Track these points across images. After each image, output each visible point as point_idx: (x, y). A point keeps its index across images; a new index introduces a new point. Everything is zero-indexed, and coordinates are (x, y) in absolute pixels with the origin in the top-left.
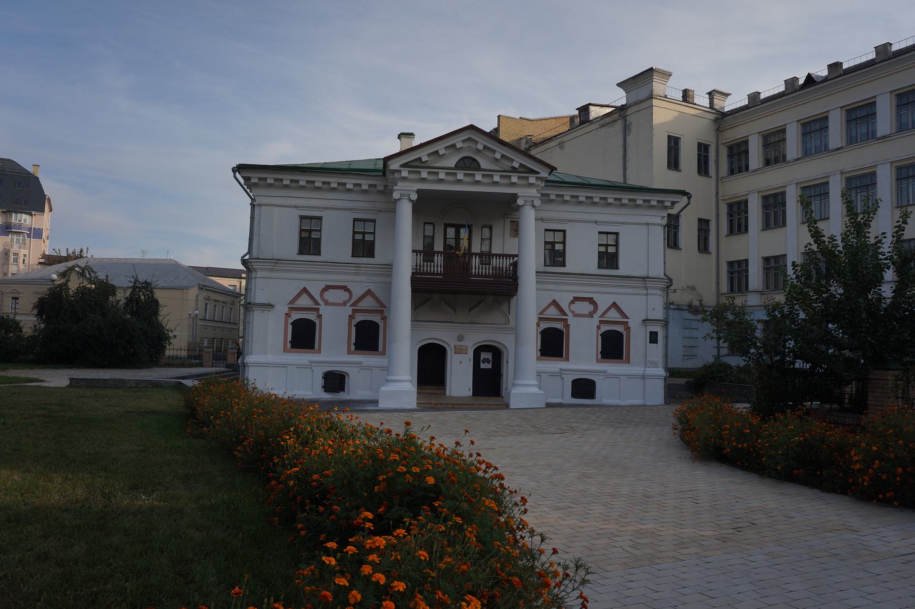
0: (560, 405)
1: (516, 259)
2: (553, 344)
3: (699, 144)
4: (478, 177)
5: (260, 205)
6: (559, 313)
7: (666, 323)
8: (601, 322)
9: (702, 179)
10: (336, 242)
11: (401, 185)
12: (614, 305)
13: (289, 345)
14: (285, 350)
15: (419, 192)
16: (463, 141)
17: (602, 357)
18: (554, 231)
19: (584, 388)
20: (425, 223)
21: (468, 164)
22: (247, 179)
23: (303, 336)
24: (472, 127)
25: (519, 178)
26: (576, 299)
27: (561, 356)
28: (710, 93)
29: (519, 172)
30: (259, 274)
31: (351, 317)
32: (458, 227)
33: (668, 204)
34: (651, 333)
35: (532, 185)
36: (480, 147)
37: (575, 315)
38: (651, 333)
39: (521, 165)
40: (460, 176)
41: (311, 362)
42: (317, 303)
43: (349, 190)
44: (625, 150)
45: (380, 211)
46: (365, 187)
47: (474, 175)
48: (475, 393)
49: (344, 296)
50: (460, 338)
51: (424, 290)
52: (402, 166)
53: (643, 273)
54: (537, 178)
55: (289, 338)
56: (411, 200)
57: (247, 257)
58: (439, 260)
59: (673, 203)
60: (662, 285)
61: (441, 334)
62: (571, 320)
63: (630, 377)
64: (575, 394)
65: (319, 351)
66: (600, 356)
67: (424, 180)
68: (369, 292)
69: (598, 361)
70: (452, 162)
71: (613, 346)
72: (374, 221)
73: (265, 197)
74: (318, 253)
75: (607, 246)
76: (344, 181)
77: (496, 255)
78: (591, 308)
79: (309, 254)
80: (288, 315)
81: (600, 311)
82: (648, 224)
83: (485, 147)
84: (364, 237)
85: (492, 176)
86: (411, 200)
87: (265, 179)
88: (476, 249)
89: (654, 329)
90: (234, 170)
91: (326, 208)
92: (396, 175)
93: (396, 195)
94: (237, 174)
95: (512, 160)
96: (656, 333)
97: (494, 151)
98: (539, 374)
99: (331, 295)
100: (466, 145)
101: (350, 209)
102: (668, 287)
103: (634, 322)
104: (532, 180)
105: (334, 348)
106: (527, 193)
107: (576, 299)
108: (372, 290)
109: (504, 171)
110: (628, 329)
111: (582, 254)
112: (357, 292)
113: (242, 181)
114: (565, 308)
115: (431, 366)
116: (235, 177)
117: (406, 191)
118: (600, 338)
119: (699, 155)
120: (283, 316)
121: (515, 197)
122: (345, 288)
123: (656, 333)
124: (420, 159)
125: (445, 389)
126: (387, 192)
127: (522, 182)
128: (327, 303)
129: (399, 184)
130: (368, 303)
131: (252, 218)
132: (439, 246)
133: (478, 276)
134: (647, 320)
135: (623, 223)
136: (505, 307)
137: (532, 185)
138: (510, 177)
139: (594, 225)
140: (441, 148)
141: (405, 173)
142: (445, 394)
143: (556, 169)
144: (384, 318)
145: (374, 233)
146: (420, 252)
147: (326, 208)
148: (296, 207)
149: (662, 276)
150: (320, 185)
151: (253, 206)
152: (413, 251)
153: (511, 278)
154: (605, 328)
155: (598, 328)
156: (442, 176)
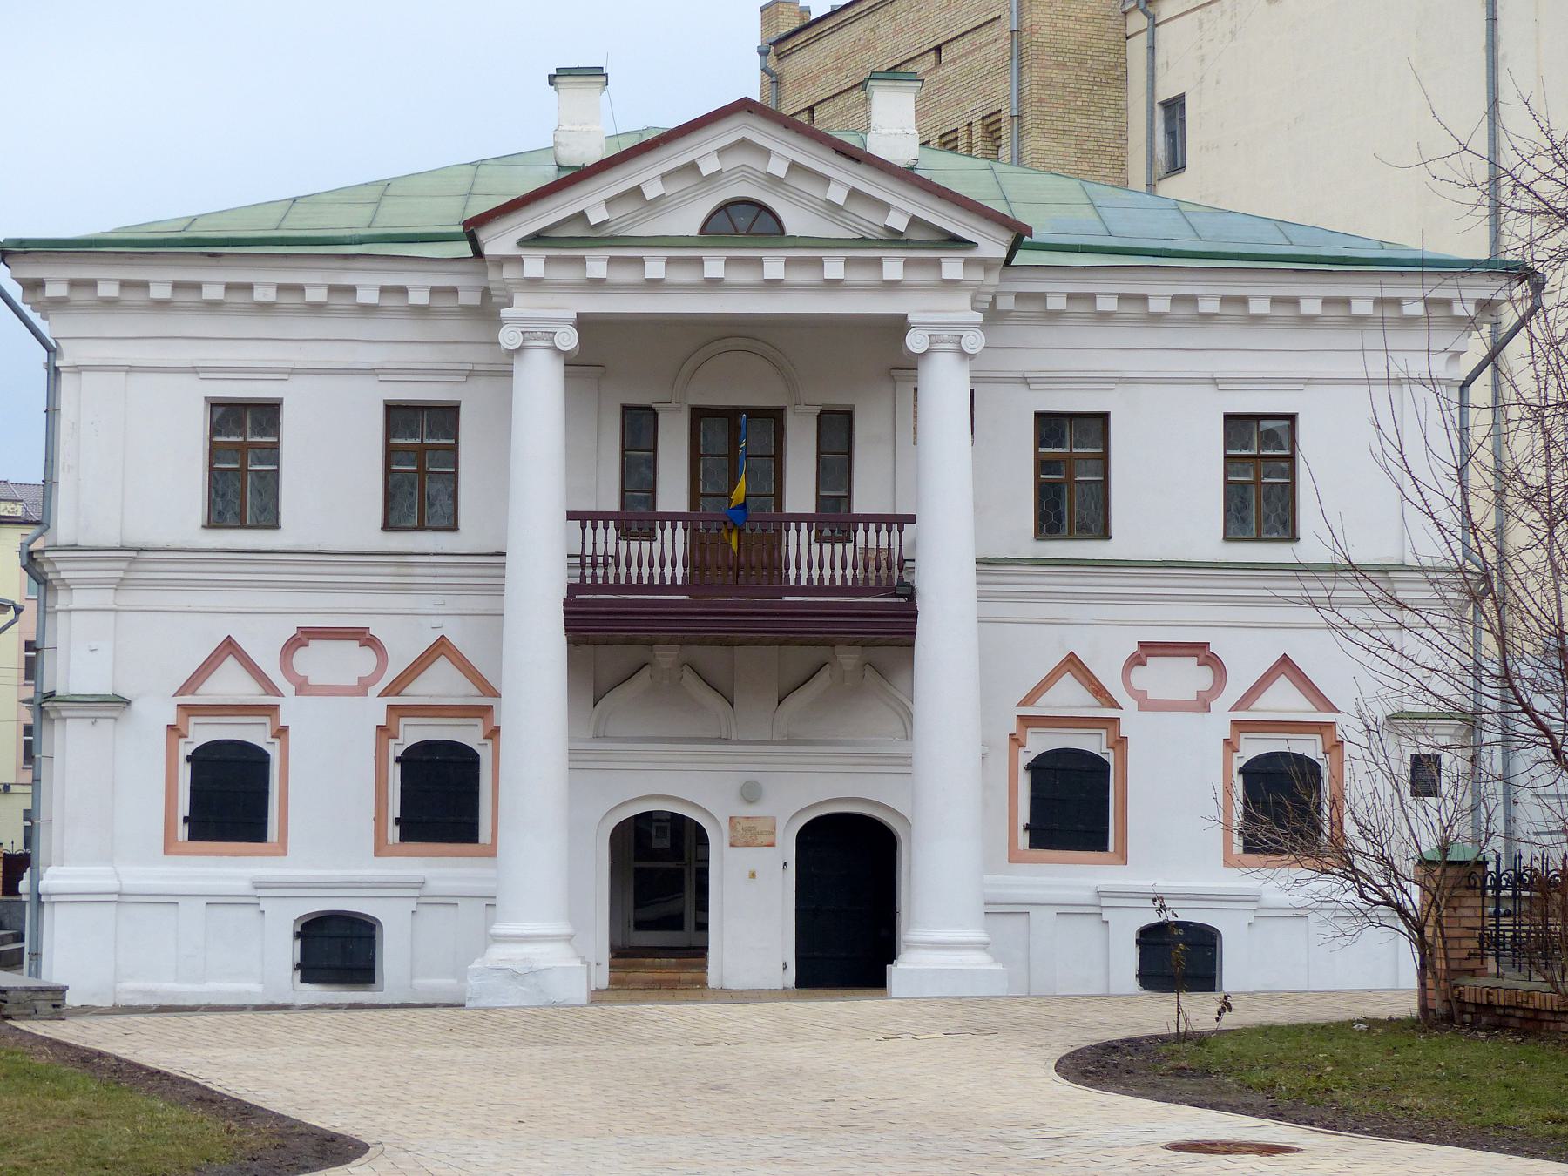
2: (1070, 804)
4: (774, 268)
5: (78, 369)
6: (1089, 699)
7: (1471, 721)
11: (523, 306)
14: (169, 847)
15: (584, 323)
21: (744, 223)
22: (33, 287)
23: (229, 796)
26: (1149, 649)
27: (1103, 846)
30: (80, 598)
35: (952, 284)
36: (778, 168)
37: (1146, 704)
39: (914, 221)
40: (714, 267)
41: (259, 884)
42: (270, 687)
44: (1492, 20)
45: (471, 374)
46: (419, 298)
47: (759, 262)
49: (359, 661)
50: (751, 794)
52: (526, 242)
54: (968, 262)
55: (184, 808)
56: (557, 351)
62: (1132, 722)
68: (441, 648)
70: (688, 219)
74: (274, 524)
76: (347, 279)
78: (1203, 677)
79: (243, 525)
86: (557, 351)
87: (92, 284)
91: (293, 371)
92: (509, 273)
93: (509, 337)
95: (886, 207)
98: (998, 910)
99: (317, 661)
100: (733, 161)
101: (372, 372)
104: (952, 268)
106: (939, 313)
107: (1149, 649)
109: (863, 242)
112: (403, 647)
114: (1112, 682)
115: (657, 885)
117: (546, 312)
121: (899, 325)
122: (361, 636)
124: (582, 215)
126: (487, 312)
127: (920, 276)
128: (303, 687)
129: (519, 299)
130: (441, 684)
131: (52, 412)
135: (1309, 381)
139: (1208, 391)
140: (648, 175)
141: (534, 265)
142: (704, 983)
143: (1028, 231)
144: (494, 733)
148: (193, 370)
150: (270, 295)
151: (54, 373)
152: (571, 516)
154: (1254, 747)
156: (655, 268)
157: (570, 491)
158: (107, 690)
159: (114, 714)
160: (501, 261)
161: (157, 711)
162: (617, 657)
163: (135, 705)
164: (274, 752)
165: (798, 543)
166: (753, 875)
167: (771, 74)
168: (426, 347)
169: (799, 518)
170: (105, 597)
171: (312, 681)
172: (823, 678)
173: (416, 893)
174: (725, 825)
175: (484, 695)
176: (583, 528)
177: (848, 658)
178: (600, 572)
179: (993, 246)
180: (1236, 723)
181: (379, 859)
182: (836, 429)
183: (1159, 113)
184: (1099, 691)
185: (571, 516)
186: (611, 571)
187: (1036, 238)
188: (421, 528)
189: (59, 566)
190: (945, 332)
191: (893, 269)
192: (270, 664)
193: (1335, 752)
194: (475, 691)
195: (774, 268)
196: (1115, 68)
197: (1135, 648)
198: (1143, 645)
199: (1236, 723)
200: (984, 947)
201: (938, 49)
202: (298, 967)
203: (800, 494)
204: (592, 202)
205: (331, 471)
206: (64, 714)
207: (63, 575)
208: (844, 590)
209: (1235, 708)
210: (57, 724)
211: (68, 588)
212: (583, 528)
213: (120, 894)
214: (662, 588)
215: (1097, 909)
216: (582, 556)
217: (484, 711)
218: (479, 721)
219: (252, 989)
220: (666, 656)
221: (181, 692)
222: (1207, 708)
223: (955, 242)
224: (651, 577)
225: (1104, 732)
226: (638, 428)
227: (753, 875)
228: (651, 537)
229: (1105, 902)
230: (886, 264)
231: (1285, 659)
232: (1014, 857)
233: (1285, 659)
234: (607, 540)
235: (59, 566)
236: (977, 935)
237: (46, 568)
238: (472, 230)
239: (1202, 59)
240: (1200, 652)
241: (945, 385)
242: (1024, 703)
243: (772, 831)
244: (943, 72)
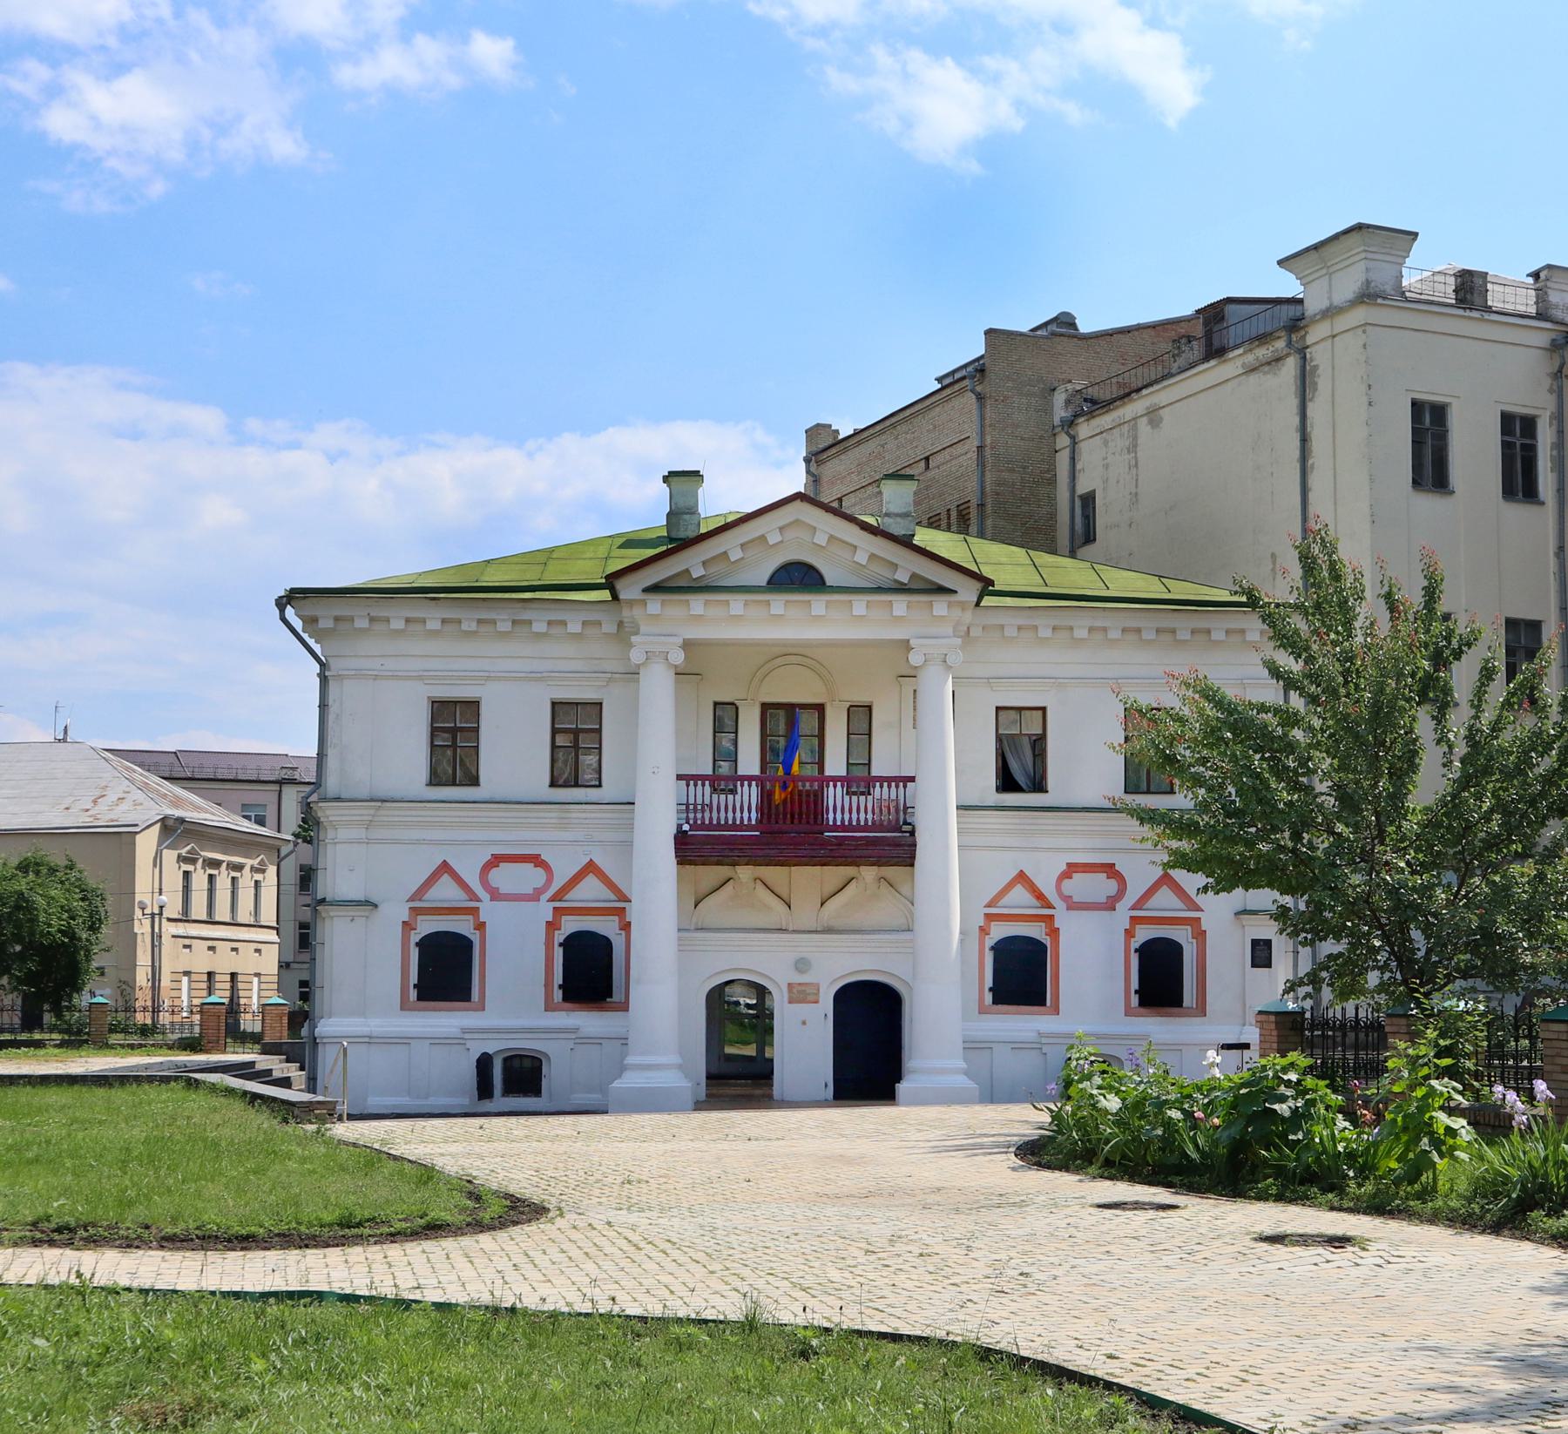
3: (1507, 419)
6: (1035, 902)
8: (1135, 920)
9: (1518, 513)
13: (413, 994)
14: (405, 1006)
17: (1142, 1004)
18: (1020, 709)
21: (798, 578)
22: (310, 622)
23: (445, 970)
27: (1042, 1003)
28: (1536, 275)
30: (343, 834)
31: (552, 926)
34: (1255, 943)
36: (821, 539)
38: (1255, 943)
39: (914, 576)
41: (464, 1031)
43: (539, 636)
44: (1304, 439)
49: (536, 877)
54: (950, 605)
55: (414, 978)
61: (766, 960)
65: (482, 1007)
66: (1135, 1000)
68: (590, 868)
74: (474, 781)
78: (1111, 887)
80: (407, 926)
93: (636, 656)
94: (290, 612)
96: (1268, 943)
99: (504, 877)
104: (940, 605)
105: (514, 998)
108: (598, 861)
113: (298, 624)
114: (1049, 890)
116: (284, 620)
119: (1506, 446)
120: (398, 930)
122: (536, 860)
123: (1268, 943)
128: (495, 895)
130: (590, 891)
131: (323, 706)
134: (1245, 912)
142: (770, 1097)
143: (991, 583)
144: (626, 927)
148: (420, 678)
154: (1144, 934)
155: (1129, 934)
157: (678, 760)
160: (631, 603)
162: (710, 874)
164: (475, 937)
165: (834, 796)
166: (804, 1023)
167: (813, 475)
169: (835, 779)
170: (361, 833)
174: (785, 989)
177: (869, 873)
178: (699, 815)
182: (861, 717)
183: (1078, 503)
184: (1040, 896)
185: (679, 777)
186: (707, 815)
187: (997, 588)
196: (1048, 471)
197: (1064, 867)
198: (1069, 865)
201: (927, 459)
203: (835, 764)
205: (514, 750)
208: (866, 828)
209: (1133, 908)
210: (327, 922)
214: (741, 827)
216: (687, 805)
217: (620, 912)
220: (745, 873)
221: (411, 899)
223: (942, 590)
226: (725, 717)
228: (733, 792)
230: (895, 605)
234: (704, 793)
238: (611, 582)
239: (1106, 467)
243: (817, 994)
244: (930, 474)
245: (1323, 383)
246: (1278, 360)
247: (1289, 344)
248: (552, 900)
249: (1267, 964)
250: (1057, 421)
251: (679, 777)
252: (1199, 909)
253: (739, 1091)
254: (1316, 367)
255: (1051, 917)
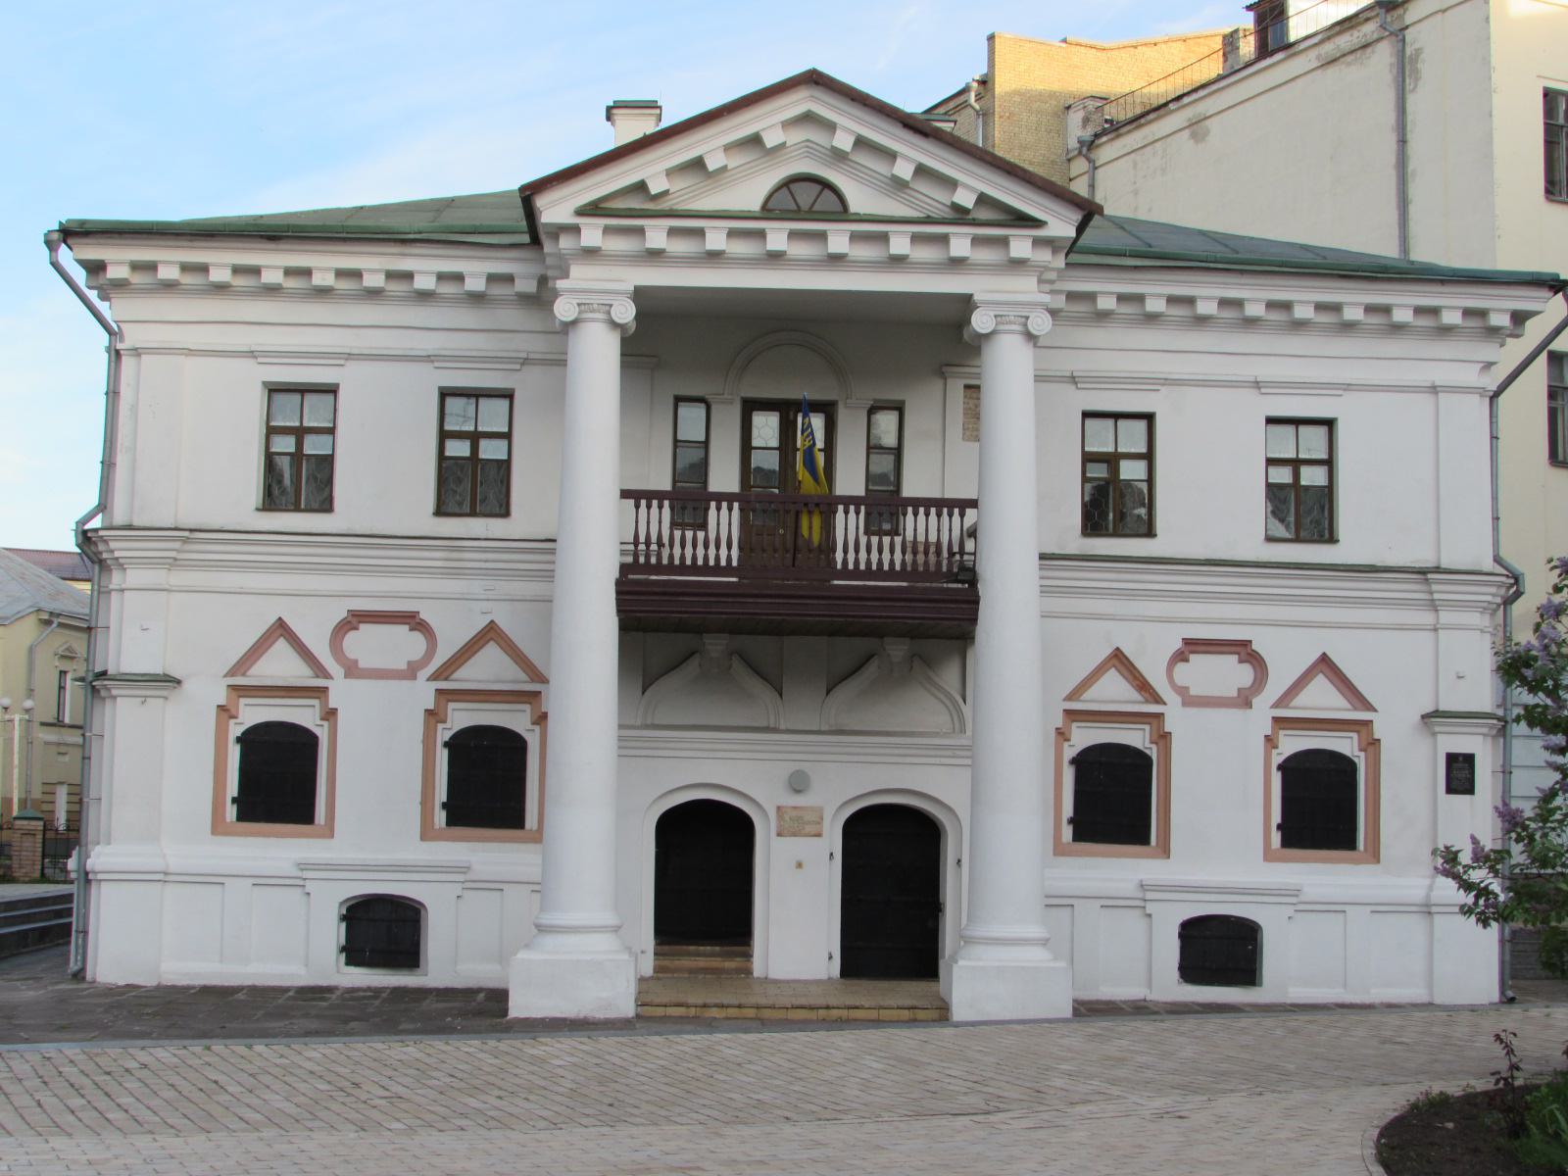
0: (1140, 1009)
1: (971, 515)
2: (1114, 798)
5: (137, 352)
6: (1135, 695)
10: (385, 468)
11: (581, 275)
12: (1325, 664)
13: (231, 812)
14: (218, 827)
16: (787, 124)
18: (1117, 416)
19: (1220, 949)
20: (679, 400)
22: (95, 268)
23: (277, 778)
24: (814, 79)
25: (977, 241)
26: (1194, 646)
29: (975, 223)
30: (134, 577)
31: (433, 716)
32: (788, 411)
33: (1501, 320)
34: (1452, 759)
35: (1018, 264)
36: (844, 141)
37: (1189, 700)
38: (1452, 759)
39: (983, 200)
41: (303, 866)
42: (320, 670)
43: (425, 296)
44: (1402, 142)
45: (526, 362)
47: (822, 236)
48: (846, 972)
50: (798, 784)
51: (670, 627)
52: (581, 212)
53: (1423, 557)
55: (232, 788)
56: (614, 325)
57: (96, 523)
58: (724, 522)
59: (1519, 318)
60: (1490, 594)
62: (1176, 718)
63: (1381, 908)
64: (1193, 969)
65: (329, 832)
66: (1276, 838)
67: (655, 255)
68: (491, 633)
69: (1269, 856)
70: (750, 192)
71: (1320, 805)
72: (508, 395)
73: (148, 319)
74: (326, 506)
75: (1296, 464)
77: (916, 503)
78: (1245, 675)
79: (297, 508)
80: (225, 712)
81: (1275, 687)
82: (1434, 389)
83: (861, 143)
84: (475, 449)
85: (884, 238)
86: (614, 325)
88: (850, 480)
89: (1461, 745)
90: (51, 245)
91: (350, 356)
92: (565, 243)
93: (564, 309)
95: (951, 184)
96: (1469, 759)
97: (891, 156)
98: (1057, 903)
99: (364, 644)
100: (796, 136)
102: (1508, 602)
103: (1395, 725)
104: (1021, 245)
107: (1193, 646)
109: (928, 221)
110: (1372, 745)
111: (1211, 494)
112: (453, 630)
113: (80, 276)
115: (702, 870)
116: (56, 265)
117: (600, 290)
118: (1276, 779)
121: (966, 304)
122: (411, 620)
123: (1469, 759)
124: (641, 187)
125: (748, 956)
126: (541, 298)
127: (985, 255)
128: (352, 670)
130: (489, 668)
131: (113, 394)
132: (724, 477)
133: (856, 574)
134: (1437, 714)
135: (1348, 387)
136: (949, 676)
137: (1018, 264)
138: (944, 239)
139: (1250, 394)
140: (709, 145)
141: (592, 234)
142: (749, 972)
144: (541, 719)
145: (507, 436)
146: (660, 496)
147: (350, 356)
148: (251, 354)
149: (1488, 564)
151: (116, 355)
153: (952, 577)
154: (1292, 744)
155: (1270, 742)
156: (716, 238)
158: (159, 671)
159: (165, 693)
161: (207, 690)
163: (186, 685)
164: (322, 733)
166: (799, 865)
168: (482, 336)
171: (362, 665)
172: (872, 669)
173: (461, 877)
175: (533, 681)
176: (637, 506)
177: (897, 650)
179: (1061, 224)
180: (1276, 720)
181: (425, 845)
184: (1143, 686)
185: (625, 494)
188: (473, 514)
189: (113, 545)
190: (1012, 313)
191: (960, 244)
192: (319, 645)
193: (1371, 749)
194: (523, 676)
195: (839, 239)
197: (1178, 645)
199: (1276, 720)
200: (1044, 942)
202: (343, 949)
204: (653, 170)
206: (114, 692)
207: (117, 554)
209: (1276, 705)
210: (108, 703)
211: (122, 567)
212: (637, 506)
213: (166, 874)
215: (1141, 901)
217: (532, 697)
218: (527, 707)
219: (291, 971)
221: (232, 673)
222: (1248, 704)
224: (706, 558)
225: (1147, 727)
227: (799, 865)
229: (1149, 895)
231: (1324, 659)
232: (1059, 850)
233: (1324, 659)
235: (113, 545)
236: (1035, 931)
237: (101, 547)
239: (1136, 193)
240: (1243, 650)
241: (1010, 370)
242: (1069, 698)
245: (1426, 68)
246: (1365, 46)
247: (1383, 27)
248: (434, 677)
249: (1468, 788)
250: (1073, 143)
251: (625, 494)
252: (1373, 709)
253: (702, 962)
254: (1418, 51)
255: (1159, 716)
